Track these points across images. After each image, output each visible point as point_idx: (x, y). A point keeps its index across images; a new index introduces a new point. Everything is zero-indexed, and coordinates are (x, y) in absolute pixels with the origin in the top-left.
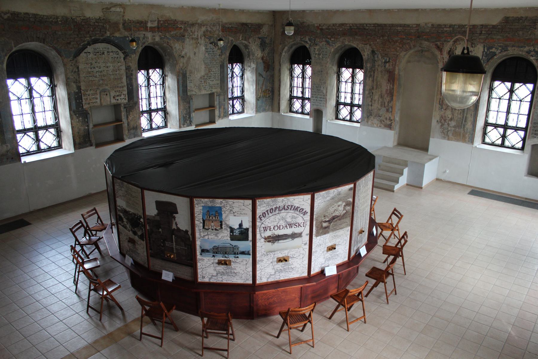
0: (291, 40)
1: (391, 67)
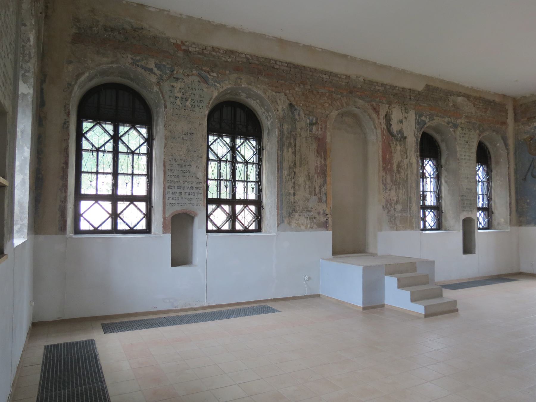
0: (105, 60)
1: (320, 132)
